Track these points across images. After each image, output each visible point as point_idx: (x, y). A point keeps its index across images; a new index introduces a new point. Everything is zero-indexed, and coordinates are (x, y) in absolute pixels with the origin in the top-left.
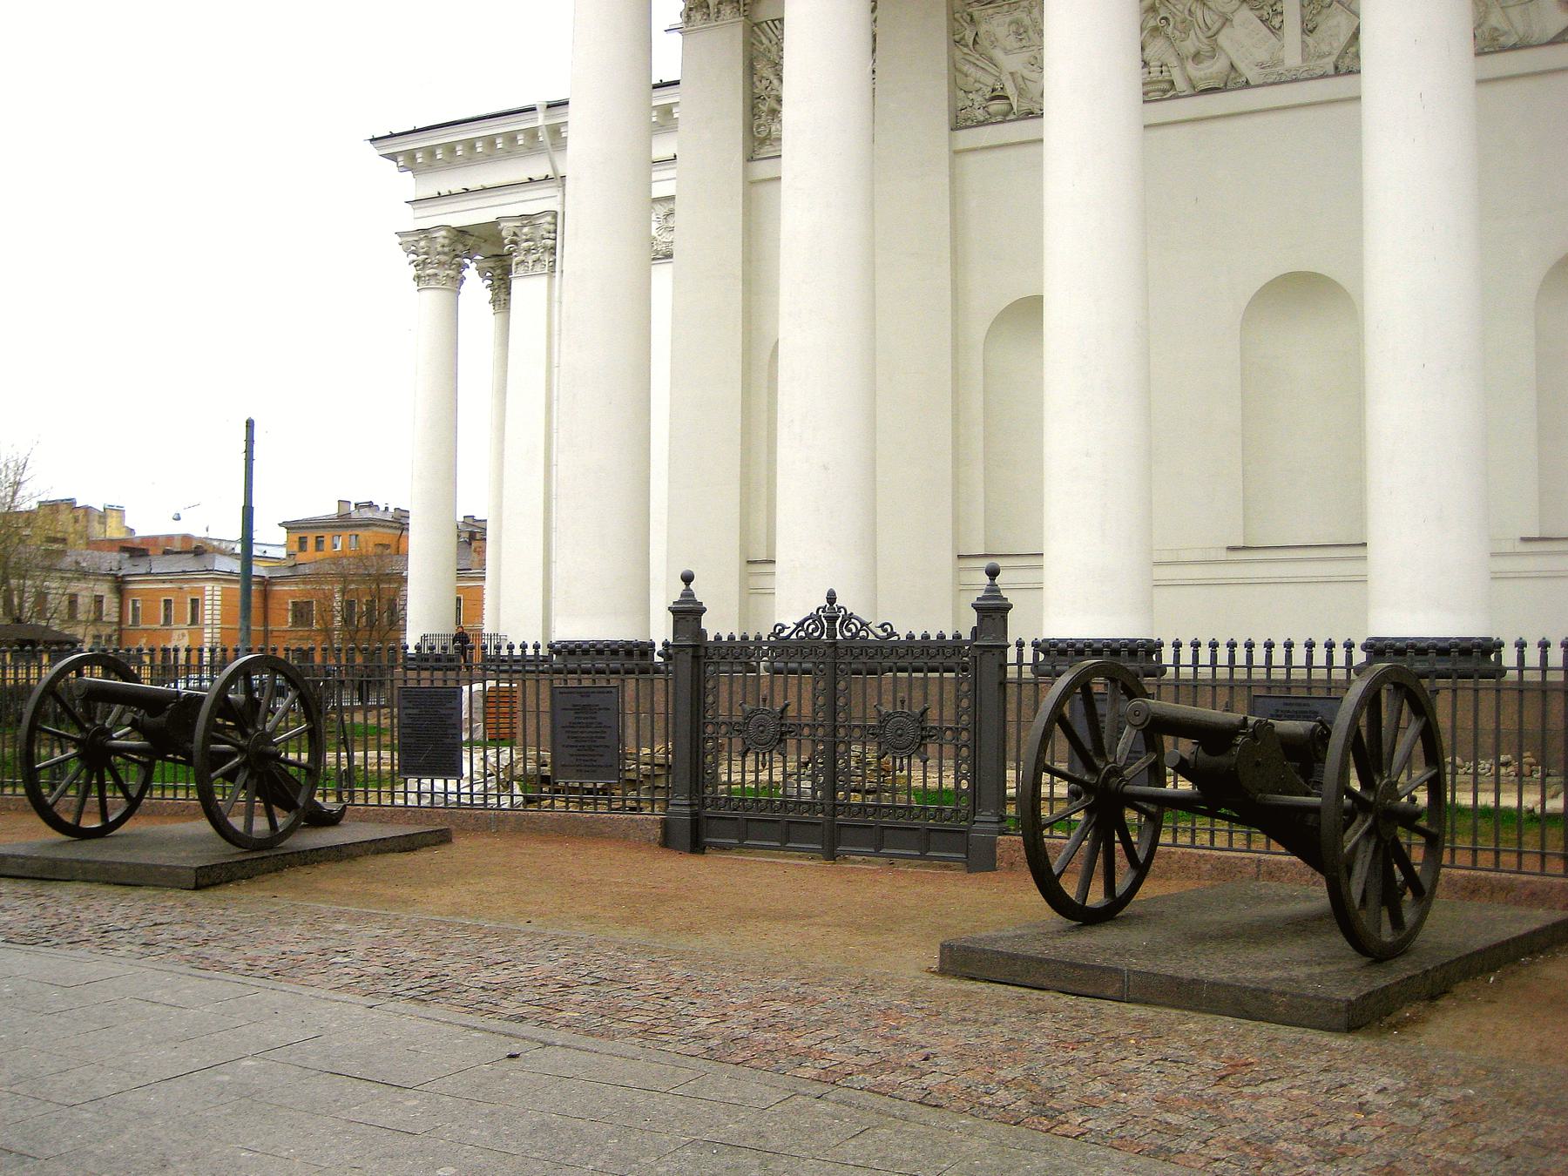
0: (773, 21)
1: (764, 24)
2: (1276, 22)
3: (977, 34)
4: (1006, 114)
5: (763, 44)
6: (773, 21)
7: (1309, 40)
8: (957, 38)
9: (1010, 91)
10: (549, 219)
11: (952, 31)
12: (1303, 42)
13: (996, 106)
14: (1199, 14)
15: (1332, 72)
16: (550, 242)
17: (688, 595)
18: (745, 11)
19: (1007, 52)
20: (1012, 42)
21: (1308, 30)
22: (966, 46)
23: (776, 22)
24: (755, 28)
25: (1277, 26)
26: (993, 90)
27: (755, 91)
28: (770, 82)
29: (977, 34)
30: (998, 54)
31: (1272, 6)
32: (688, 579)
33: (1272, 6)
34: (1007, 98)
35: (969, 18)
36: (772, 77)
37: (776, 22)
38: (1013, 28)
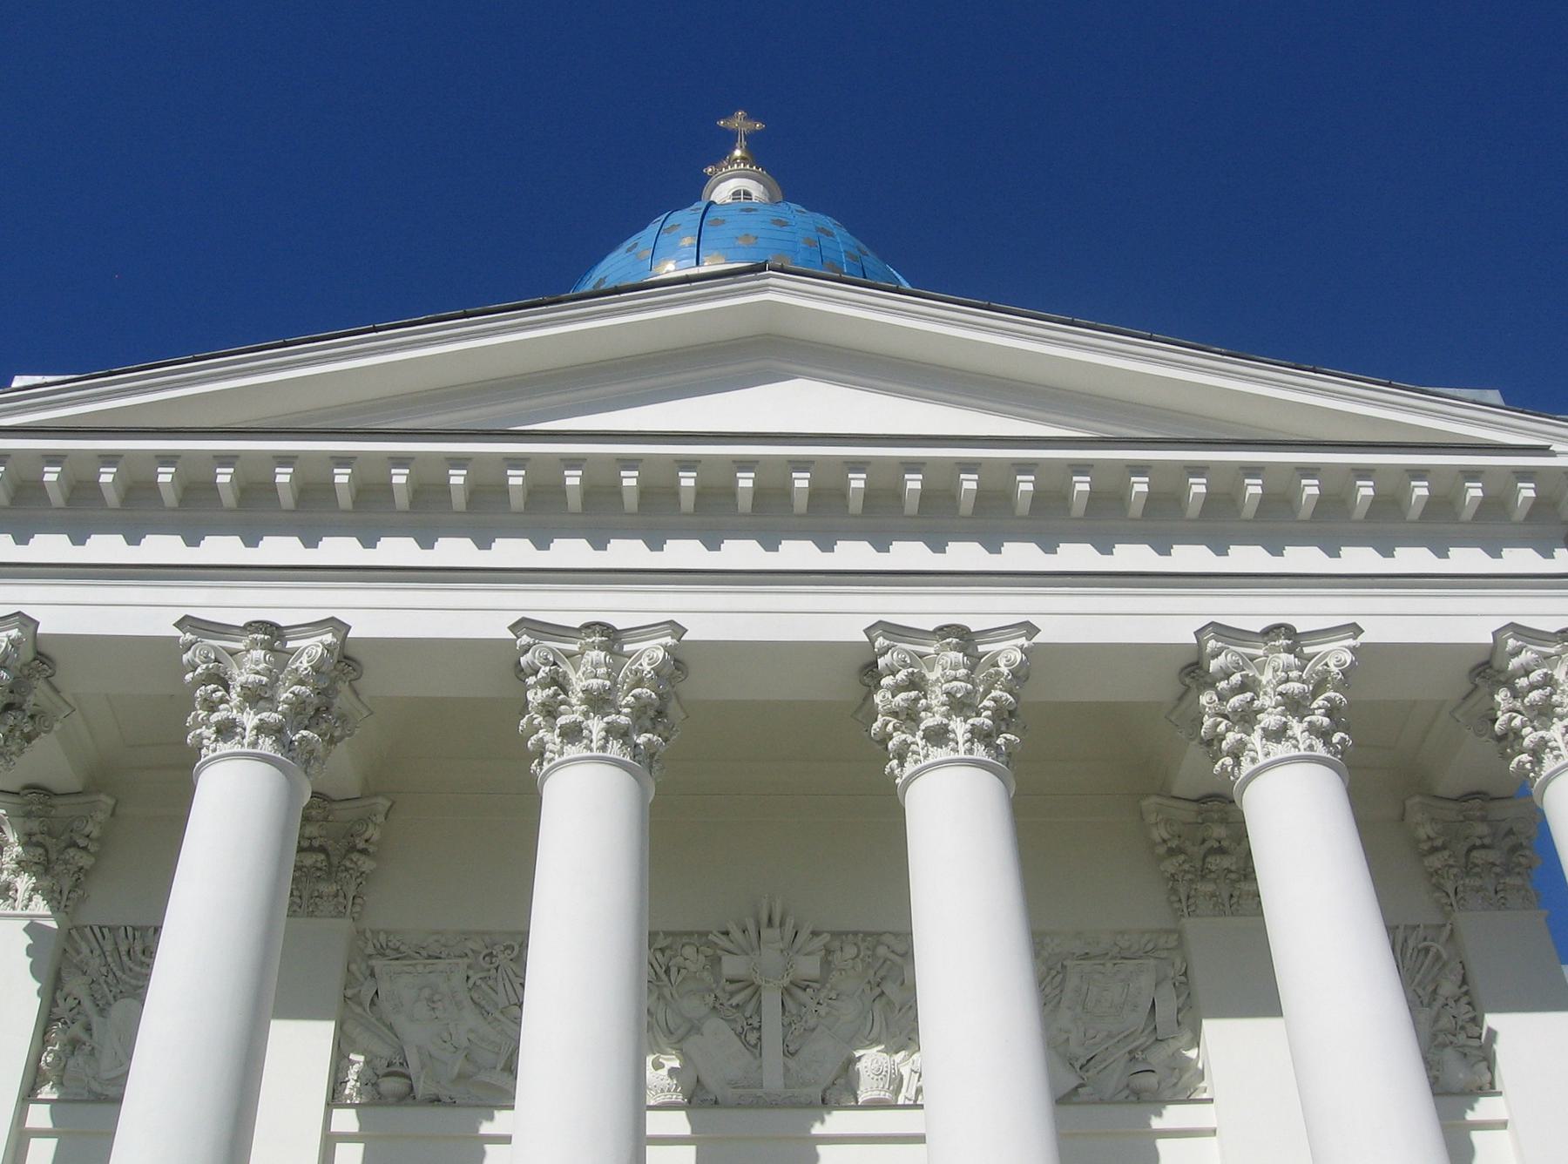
0: (100, 928)
1: (88, 930)
2: (752, 1038)
5: (78, 953)
7: (792, 1063)
8: (349, 993)
11: (350, 980)
18: (66, 906)
21: (789, 1053)
22: (360, 1004)
23: (106, 931)
24: (74, 932)
25: (753, 1042)
27: (55, 1010)
28: (79, 1002)
29: (377, 992)
31: (747, 1019)
34: (408, 1077)
35: (368, 973)
38: (426, 993)
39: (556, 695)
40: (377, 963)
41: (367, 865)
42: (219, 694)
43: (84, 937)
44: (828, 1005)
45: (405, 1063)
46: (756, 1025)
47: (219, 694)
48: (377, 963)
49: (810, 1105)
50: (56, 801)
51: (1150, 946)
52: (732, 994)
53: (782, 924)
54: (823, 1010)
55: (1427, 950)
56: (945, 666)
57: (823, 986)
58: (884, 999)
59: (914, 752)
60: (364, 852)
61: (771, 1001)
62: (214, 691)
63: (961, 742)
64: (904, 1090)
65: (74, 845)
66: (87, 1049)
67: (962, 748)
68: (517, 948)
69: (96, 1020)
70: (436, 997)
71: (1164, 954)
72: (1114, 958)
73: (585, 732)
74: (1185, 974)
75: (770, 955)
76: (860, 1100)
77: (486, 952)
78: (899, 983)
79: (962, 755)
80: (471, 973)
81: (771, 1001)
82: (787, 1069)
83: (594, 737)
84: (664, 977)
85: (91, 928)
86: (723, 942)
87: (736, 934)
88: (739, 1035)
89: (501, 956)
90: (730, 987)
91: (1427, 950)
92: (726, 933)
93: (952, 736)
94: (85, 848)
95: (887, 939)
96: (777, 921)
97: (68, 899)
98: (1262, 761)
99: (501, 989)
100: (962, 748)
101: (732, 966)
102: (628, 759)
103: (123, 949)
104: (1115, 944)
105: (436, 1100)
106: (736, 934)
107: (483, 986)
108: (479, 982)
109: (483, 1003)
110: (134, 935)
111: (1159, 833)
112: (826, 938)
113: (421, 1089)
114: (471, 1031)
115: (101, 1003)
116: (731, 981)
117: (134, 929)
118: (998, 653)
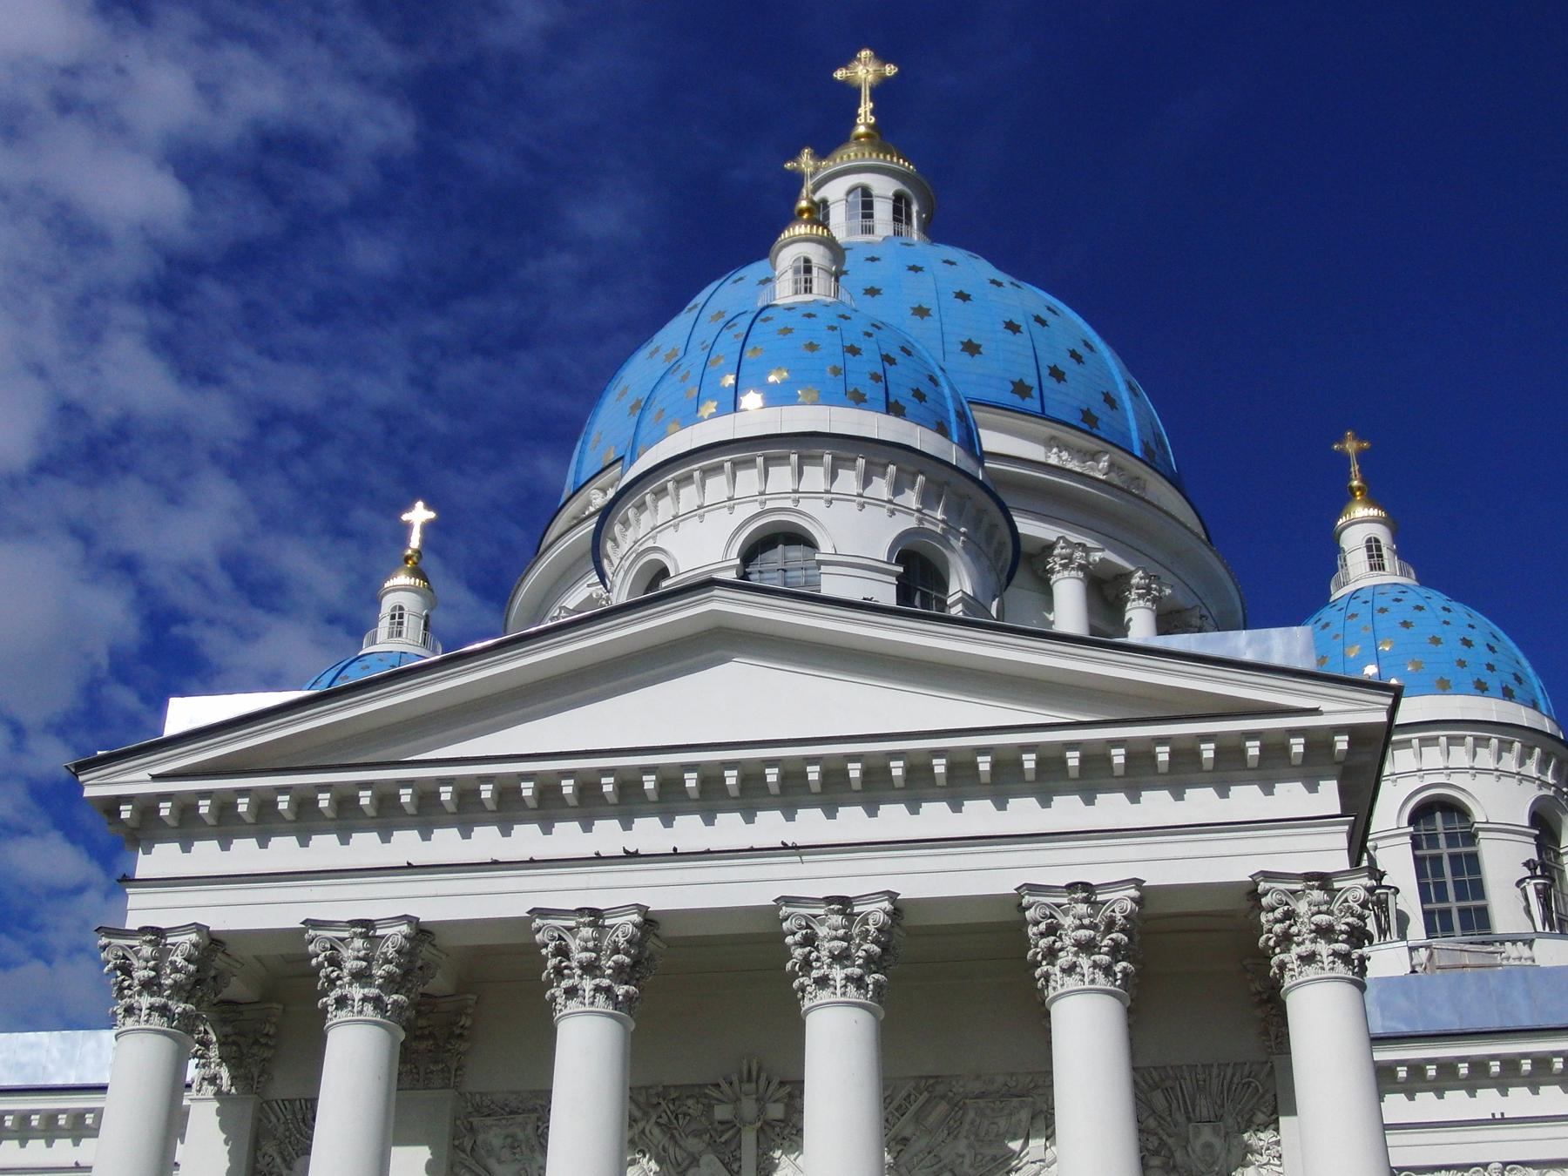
0: (283, 1101)
1: (275, 1105)
3: (475, 1142)
5: (270, 1122)
6: (283, 1101)
8: (457, 1142)
14: (671, 1151)
18: (257, 1088)
19: (500, 1161)
20: (506, 1154)
22: (464, 1151)
23: (286, 1103)
25: (736, 1169)
28: (273, 1159)
29: (475, 1142)
31: (732, 1152)
33: (732, 1152)
35: (469, 1126)
36: (275, 1155)
38: (509, 1141)
39: (561, 962)
40: (476, 1121)
41: (464, 1047)
42: (335, 974)
43: (271, 1108)
47: (335, 974)
48: (476, 1121)
50: (241, 1008)
51: (1032, 1085)
52: (723, 1132)
53: (758, 1077)
55: (1249, 1083)
56: (829, 928)
60: (460, 1036)
61: (749, 1137)
62: (333, 971)
65: (256, 1042)
72: (1003, 1095)
73: (580, 992)
75: (749, 1107)
80: (540, 1124)
81: (749, 1137)
84: (675, 1121)
86: (714, 1093)
87: (725, 1087)
90: (720, 1128)
91: (1249, 1083)
92: (717, 1086)
93: (832, 983)
94: (266, 1045)
97: (258, 1082)
98: (1060, 990)
100: (839, 991)
101: (722, 1112)
106: (725, 1087)
115: (288, 1158)
116: (721, 1123)
118: (869, 914)
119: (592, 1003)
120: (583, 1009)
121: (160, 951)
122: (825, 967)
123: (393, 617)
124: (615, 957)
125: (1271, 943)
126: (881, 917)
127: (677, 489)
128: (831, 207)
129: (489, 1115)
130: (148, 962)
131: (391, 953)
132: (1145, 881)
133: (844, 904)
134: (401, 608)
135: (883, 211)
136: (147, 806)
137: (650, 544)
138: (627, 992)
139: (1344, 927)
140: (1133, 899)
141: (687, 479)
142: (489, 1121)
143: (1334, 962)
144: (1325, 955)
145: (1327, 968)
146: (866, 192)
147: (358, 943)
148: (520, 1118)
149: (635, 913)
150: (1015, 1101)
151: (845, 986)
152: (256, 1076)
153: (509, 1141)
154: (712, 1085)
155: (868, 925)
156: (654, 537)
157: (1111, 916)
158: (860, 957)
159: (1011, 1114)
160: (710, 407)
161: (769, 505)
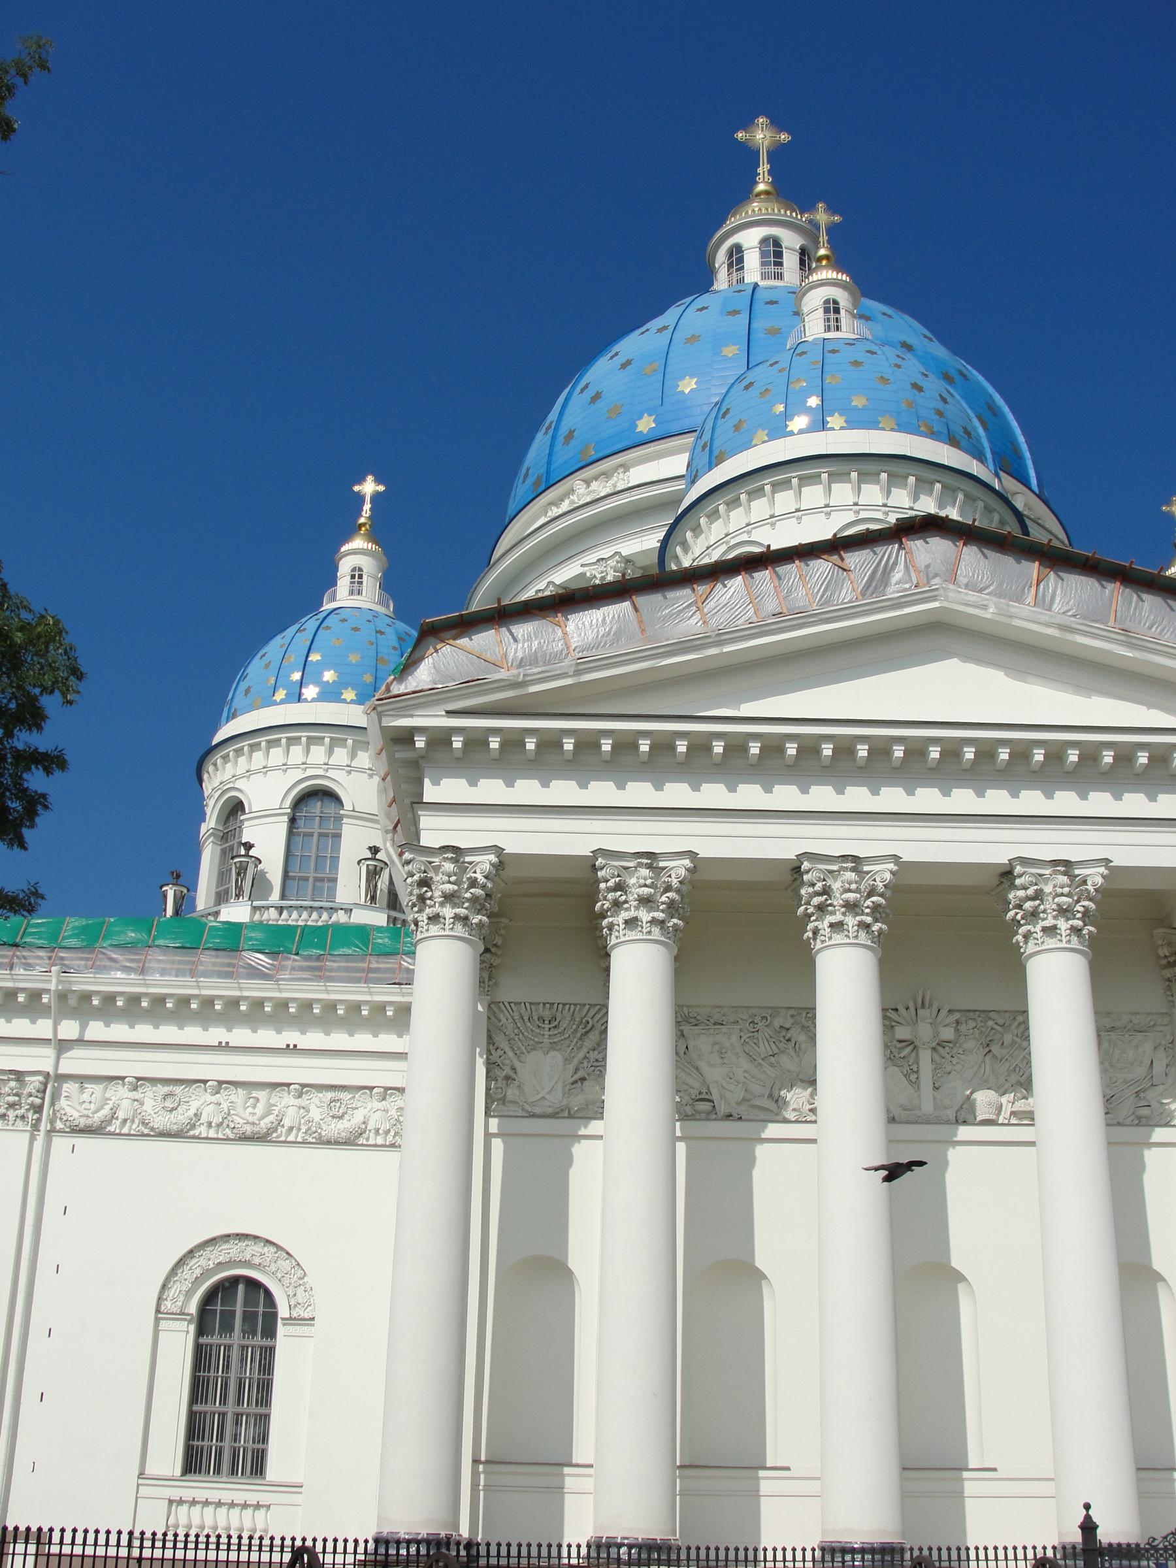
0: (509, 1003)
1: (501, 1005)
2: (913, 1077)
4: (708, 1113)
5: (500, 1021)
6: (509, 1003)
7: (937, 1094)
9: (715, 1096)
10: (41, 1078)
12: (933, 1096)
13: (704, 1106)
15: (954, 1121)
16: (38, 1101)
17: (1088, 1518)
19: (710, 1065)
20: (715, 1058)
21: (936, 1088)
23: (512, 1005)
24: (492, 1006)
25: (914, 1080)
26: (700, 1093)
27: (490, 1057)
29: (687, 1047)
30: (703, 1066)
32: (1087, 1507)
34: (712, 1101)
36: (507, 1049)
37: (512, 1005)
38: (717, 1047)
39: (826, 900)
43: (499, 1008)
44: (958, 1058)
45: (709, 1092)
46: (915, 1069)
49: (947, 1122)
51: (1152, 1023)
53: (930, 1006)
54: (955, 1061)
57: (955, 1045)
58: (991, 1054)
59: (1035, 938)
61: (925, 1056)
62: (621, 895)
63: (1064, 934)
64: (1003, 1113)
66: (516, 1083)
67: (1064, 940)
68: (769, 1018)
69: (517, 1064)
70: (723, 1051)
71: (1161, 1028)
72: (1129, 1030)
73: (845, 927)
74: (1172, 1043)
75: (925, 1031)
76: (978, 1119)
77: (750, 1020)
78: (1000, 1044)
79: (1064, 945)
80: (742, 1034)
81: (925, 1056)
82: (935, 1098)
83: (850, 929)
85: (503, 1003)
88: (905, 1076)
89: (760, 1024)
92: (896, 1010)
93: (1059, 931)
95: (992, 1015)
96: (927, 1003)
97: (489, 986)
99: (761, 1043)
101: (902, 1032)
102: (869, 943)
103: (526, 1018)
104: (1131, 1021)
105: (729, 1116)
106: (902, 1010)
107: (750, 1043)
108: (747, 1040)
109: (751, 1054)
110: (531, 1009)
111: (1164, 951)
112: (957, 1016)
113: (722, 1109)
114: (745, 1071)
115: (518, 1052)
116: (900, 1041)
117: (530, 1003)
119: (856, 937)
120: (848, 941)
121: (459, 867)
122: (633, 909)
123: (353, 577)
124: (472, 890)
125: (1019, 917)
126: (683, 872)
127: (773, 492)
128: (745, 252)
129: (696, 1025)
130: (449, 877)
131: (675, 882)
132: (1112, 862)
133: (1067, 866)
134: (360, 569)
135: (790, 260)
136: (440, 739)
137: (745, 537)
138: (881, 928)
139: (1081, 909)
140: (891, 872)
141: (785, 484)
142: (697, 1030)
143: (1070, 935)
144: (1063, 930)
145: (1064, 940)
146: (777, 243)
147: (645, 872)
148: (724, 1029)
149: (891, 862)
150: (1140, 1036)
151: (1070, 935)
152: (486, 980)
153: (717, 1047)
154: (892, 1009)
155: (1087, 885)
156: (749, 532)
157: (874, 885)
158: (1078, 912)
159: (1137, 1047)
160: (800, 422)
161: (863, 515)
